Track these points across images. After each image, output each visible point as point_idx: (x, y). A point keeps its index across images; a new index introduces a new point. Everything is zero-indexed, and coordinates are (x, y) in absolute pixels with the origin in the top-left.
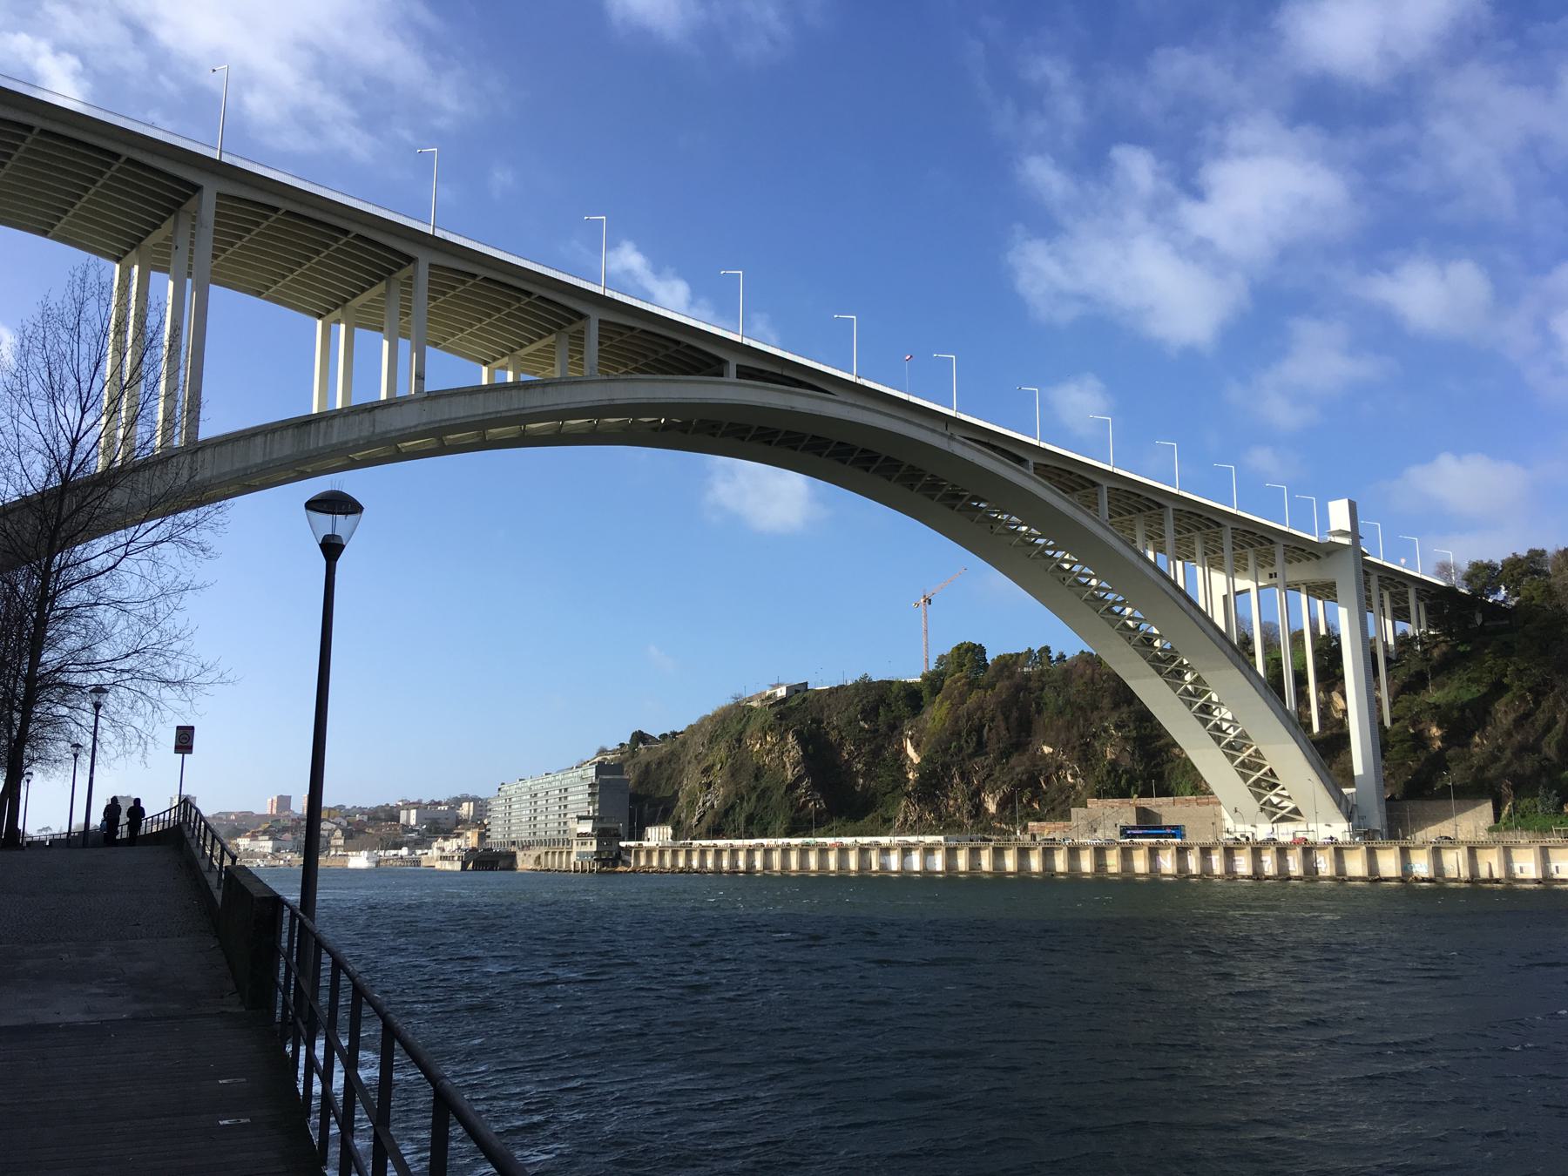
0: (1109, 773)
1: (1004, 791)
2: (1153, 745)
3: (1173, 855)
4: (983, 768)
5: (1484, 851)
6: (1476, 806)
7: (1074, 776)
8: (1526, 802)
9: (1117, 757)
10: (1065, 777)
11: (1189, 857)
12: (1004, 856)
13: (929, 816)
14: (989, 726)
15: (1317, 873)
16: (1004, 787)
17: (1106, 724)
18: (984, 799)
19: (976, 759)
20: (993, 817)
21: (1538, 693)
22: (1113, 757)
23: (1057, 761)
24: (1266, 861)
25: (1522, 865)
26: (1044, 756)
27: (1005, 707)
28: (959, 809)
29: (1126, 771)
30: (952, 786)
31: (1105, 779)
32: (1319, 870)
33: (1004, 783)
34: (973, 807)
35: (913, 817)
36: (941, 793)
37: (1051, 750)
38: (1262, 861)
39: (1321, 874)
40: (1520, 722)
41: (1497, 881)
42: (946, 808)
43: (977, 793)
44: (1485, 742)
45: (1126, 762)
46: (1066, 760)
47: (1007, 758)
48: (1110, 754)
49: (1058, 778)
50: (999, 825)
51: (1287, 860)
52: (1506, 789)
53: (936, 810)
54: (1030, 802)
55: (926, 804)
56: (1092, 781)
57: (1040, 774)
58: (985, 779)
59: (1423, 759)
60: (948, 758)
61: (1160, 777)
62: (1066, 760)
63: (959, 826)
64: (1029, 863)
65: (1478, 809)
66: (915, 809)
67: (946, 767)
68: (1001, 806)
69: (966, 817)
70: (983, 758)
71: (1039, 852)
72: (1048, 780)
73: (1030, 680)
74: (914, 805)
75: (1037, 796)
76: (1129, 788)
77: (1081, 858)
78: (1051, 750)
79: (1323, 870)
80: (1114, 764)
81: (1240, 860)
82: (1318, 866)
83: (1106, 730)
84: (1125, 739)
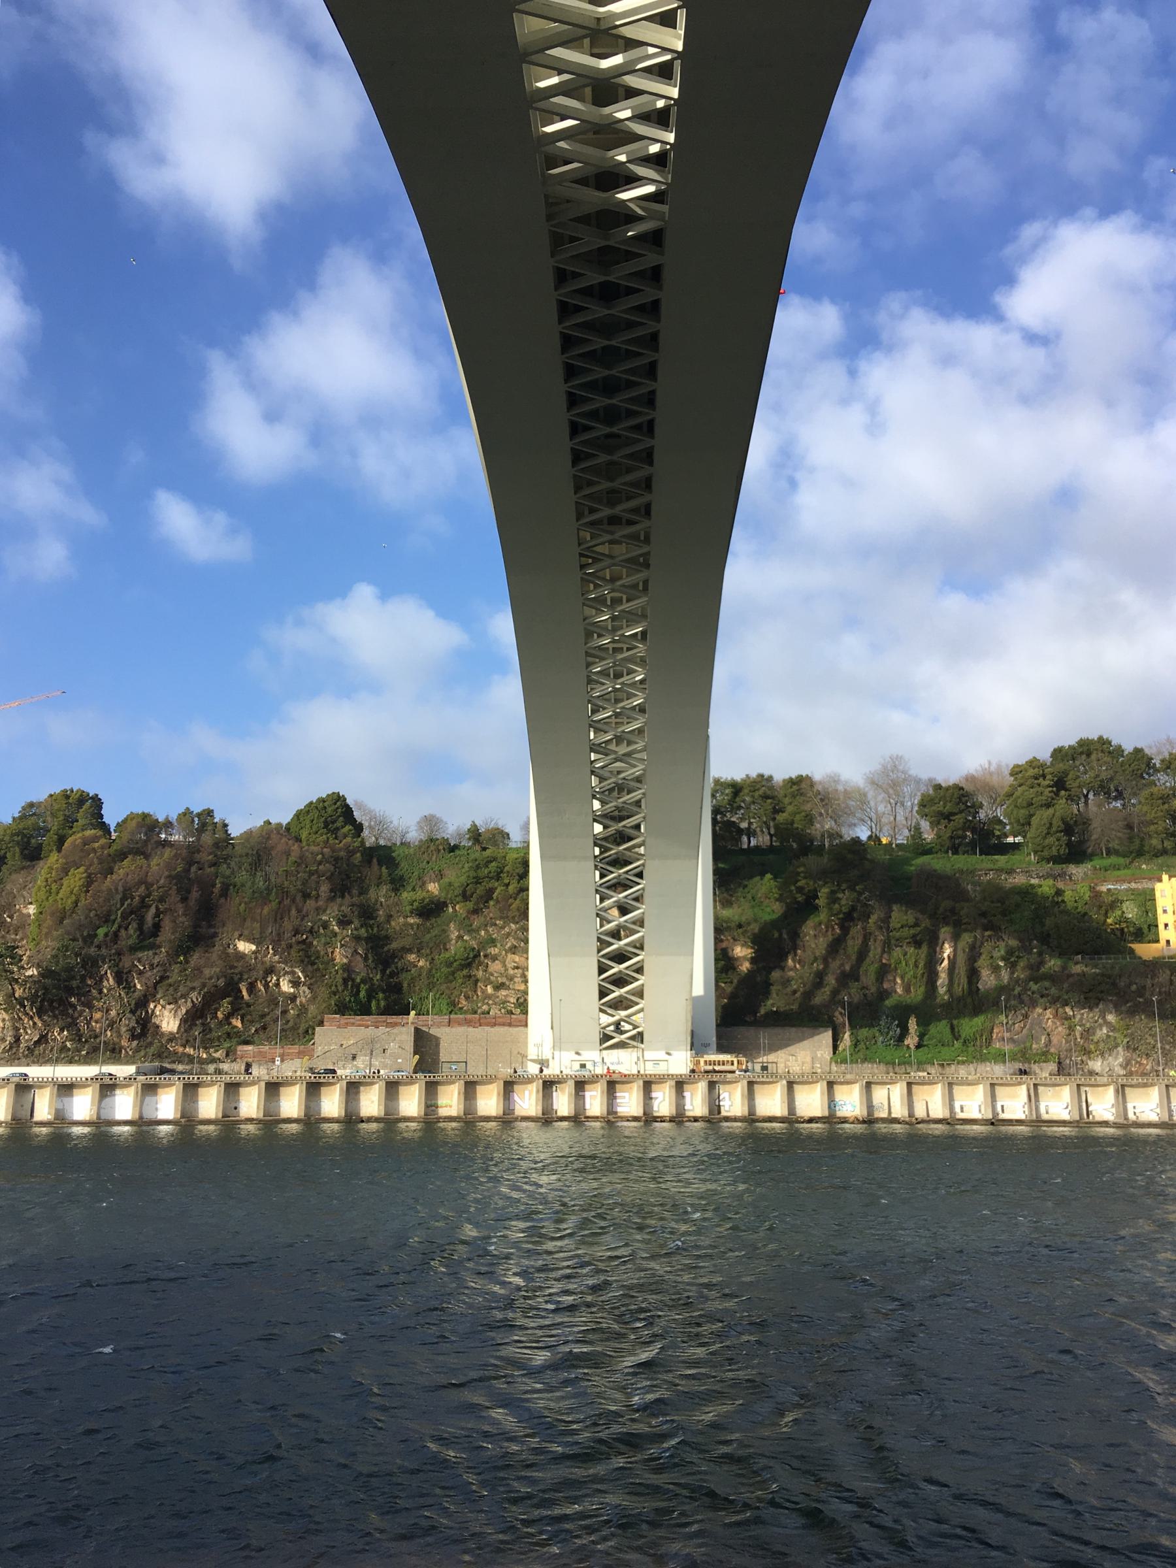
0: (345, 981)
1: (192, 1001)
2: (386, 949)
3: (538, 1091)
4: (152, 967)
5: (921, 1087)
6: (812, 1036)
7: (295, 983)
8: (864, 1033)
9: (350, 961)
10: (278, 985)
11: (554, 1093)
13: (59, 1035)
14: (157, 908)
15: (719, 1112)
16: (194, 995)
17: (324, 918)
18: (153, 1011)
19: (140, 955)
20: (172, 1038)
21: (847, 919)
22: (345, 961)
23: (263, 963)
24: (656, 1098)
25: (962, 1103)
26: (241, 956)
27: (182, 882)
28: (111, 1025)
29: (363, 981)
30: (101, 992)
31: (340, 989)
32: (722, 1108)
33: (193, 989)
34: (137, 1022)
35: (30, 1036)
36: (79, 1000)
37: (254, 947)
38: (651, 1098)
39: (724, 1113)
40: (835, 947)
41: (896, 1121)
42: (88, 1023)
43: (143, 1003)
44: (798, 966)
45: (360, 968)
46: (279, 962)
47: (185, 955)
48: (340, 956)
49: (266, 986)
50: (181, 1049)
51: (684, 1097)
52: (840, 1017)
53: (72, 1025)
54: (228, 1017)
55: (55, 1017)
56: (323, 992)
57: (241, 980)
58: (157, 983)
59: (735, 981)
60: (93, 951)
61: (397, 989)
63: (113, 1051)
64: (319, 1106)
65: (816, 1038)
66: (35, 1024)
67: (91, 965)
68: (189, 1021)
69: (126, 1035)
70: (151, 953)
71: (341, 1089)
72: (252, 988)
73: (199, 851)
74: (32, 1018)
75: (239, 1009)
76: (369, 1001)
77: (400, 1096)
78: (254, 947)
79: (727, 1108)
80: (347, 968)
81: (624, 1097)
82: (721, 1103)
83: (325, 925)
84: (357, 938)
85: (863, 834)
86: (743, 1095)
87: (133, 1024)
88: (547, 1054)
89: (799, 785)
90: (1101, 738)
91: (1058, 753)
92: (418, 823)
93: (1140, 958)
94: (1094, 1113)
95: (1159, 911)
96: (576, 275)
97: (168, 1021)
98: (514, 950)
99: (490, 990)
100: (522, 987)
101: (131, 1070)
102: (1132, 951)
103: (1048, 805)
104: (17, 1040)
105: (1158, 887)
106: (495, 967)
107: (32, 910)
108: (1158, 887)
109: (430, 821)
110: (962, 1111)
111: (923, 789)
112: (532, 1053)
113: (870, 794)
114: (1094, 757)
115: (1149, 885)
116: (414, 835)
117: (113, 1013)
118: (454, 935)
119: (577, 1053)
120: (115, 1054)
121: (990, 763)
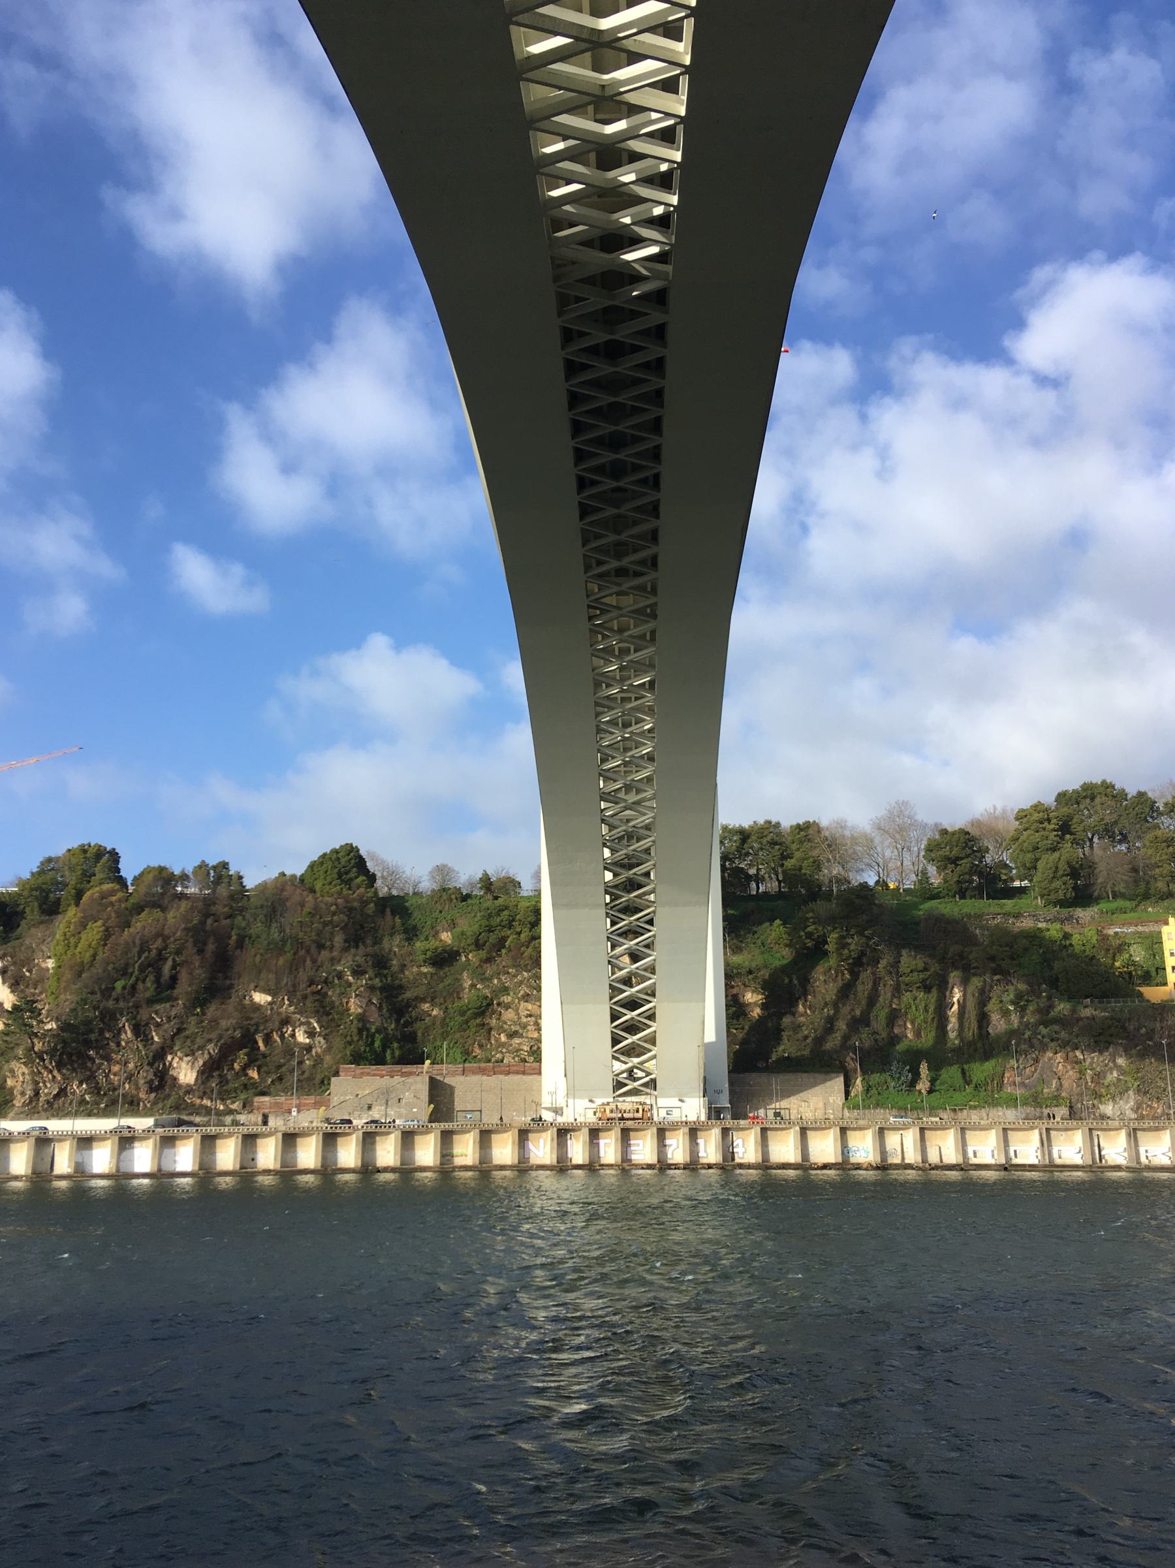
0: (360, 1031)
1: (209, 1053)
2: (400, 998)
3: (552, 1140)
4: (169, 1019)
5: (934, 1132)
6: (824, 1081)
7: (311, 1034)
8: (876, 1078)
9: (365, 1011)
10: (293, 1035)
11: (569, 1142)
12: (295, 1146)
13: (78, 1089)
14: (174, 960)
15: (733, 1159)
16: (210, 1047)
17: (339, 968)
18: (170, 1063)
19: (157, 1007)
20: (189, 1090)
21: (857, 965)
22: (360, 1010)
23: (279, 1014)
24: (670, 1145)
25: (975, 1148)
26: (257, 1007)
27: (198, 934)
28: (129, 1078)
29: (378, 1031)
30: (118, 1045)
31: (355, 1039)
32: (736, 1155)
33: (210, 1041)
34: (155, 1075)
35: (49, 1089)
36: (97, 1053)
37: (269, 998)
38: (665, 1146)
39: (737, 1160)
40: (846, 991)
41: (909, 1167)
42: (107, 1076)
43: (160, 1055)
44: (808, 1011)
45: (375, 1019)
46: (294, 1013)
47: (201, 1006)
48: (355, 1006)
49: (282, 1037)
50: (198, 1101)
51: (697, 1144)
52: (851, 1062)
53: (90, 1078)
54: (244, 1068)
55: (74, 1070)
56: (338, 1042)
57: (257, 1031)
58: (175, 1035)
59: (747, 1027)
60: (110, 1004)
61: (411, 1038)
62: (294, 1013)
63: (131, 1103)
65: (828, 1084)
66: (54, 1077)
67: (109, 1018)
68: (205, 1073)
69: (144, 1088)
70: (168, 1005)
72: (268, 1039)
73: (214, 904)
74: (51, 1072)
75: (256, 1060)
76: (384, 1051)
77: (416, 1146)
78: (269, 998)
79: (741, 1155)
80: (362, 1018)
81: (638, 1145)
82: (735, 1150)
83: (340, 975)
85: (871, 879)
86: (756, 1142)
87: (151, 1076)
88: (561, 1102)
89: (806, 831)
90: (1104, 782)
91: (1062, 797)
92: (430, 873)
93: (1148, 1001)
94: (1106, 1157)
95: (1167, 954)
96: (582, 334)
97: (186, 1073)
98: (526, 998)
99: (503, 1038)
100: (536, 1035)
101: (149, 1122)
102: (1140, 995)
103: (1054, 849)
104: (37, 1094)
105: (1165, 930)
106: (509, 1015)
107: (50, 964)
108: (1165, 930)
109: (442, 871)
110: (975, 1156)
111: (929, 834)
112: (546, 1101)
113: (877, 840)
114: (1098, 800)
115: (1156, 928)
116: (427, 885)
117: (131, 1066)
118: (467, 983)
119: (591, 1101)
120: (133, 1106)
121: (995, 807)
